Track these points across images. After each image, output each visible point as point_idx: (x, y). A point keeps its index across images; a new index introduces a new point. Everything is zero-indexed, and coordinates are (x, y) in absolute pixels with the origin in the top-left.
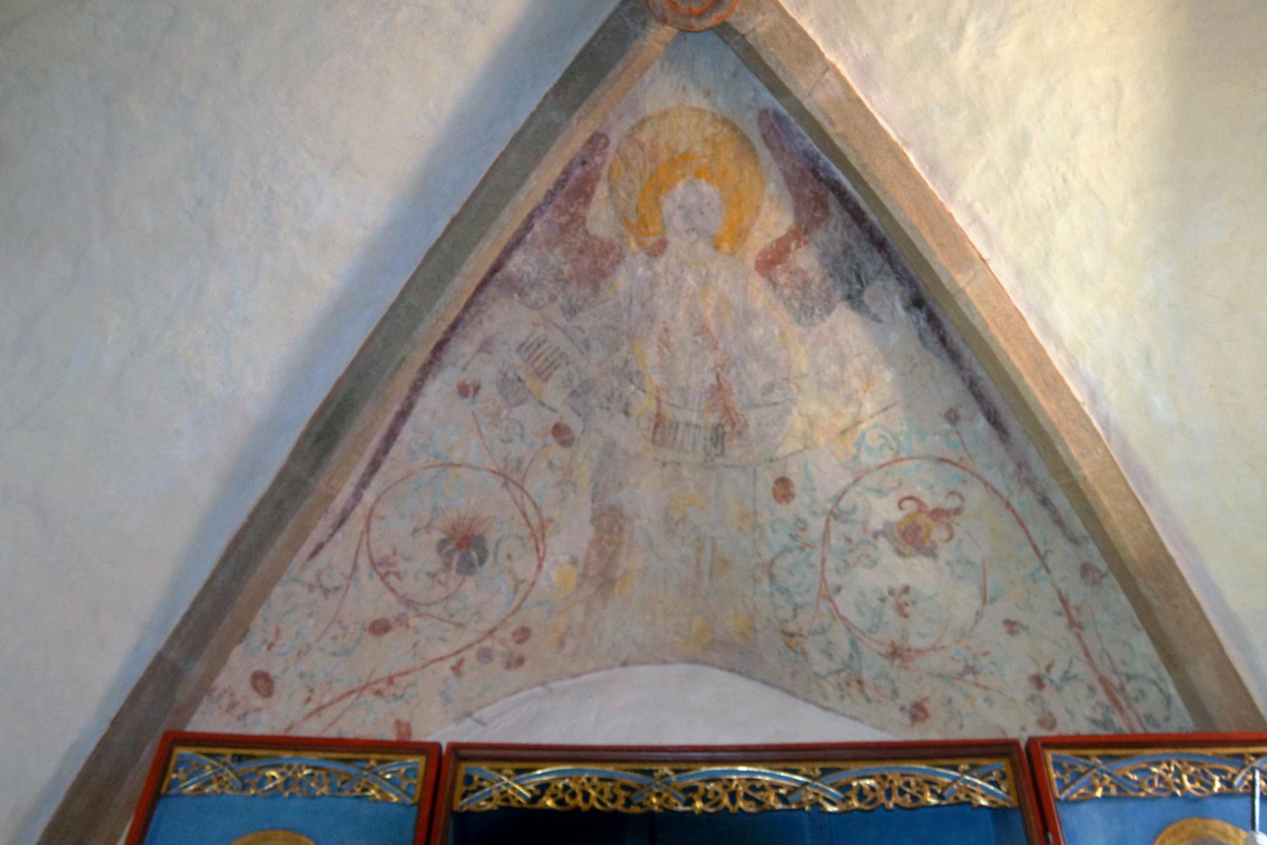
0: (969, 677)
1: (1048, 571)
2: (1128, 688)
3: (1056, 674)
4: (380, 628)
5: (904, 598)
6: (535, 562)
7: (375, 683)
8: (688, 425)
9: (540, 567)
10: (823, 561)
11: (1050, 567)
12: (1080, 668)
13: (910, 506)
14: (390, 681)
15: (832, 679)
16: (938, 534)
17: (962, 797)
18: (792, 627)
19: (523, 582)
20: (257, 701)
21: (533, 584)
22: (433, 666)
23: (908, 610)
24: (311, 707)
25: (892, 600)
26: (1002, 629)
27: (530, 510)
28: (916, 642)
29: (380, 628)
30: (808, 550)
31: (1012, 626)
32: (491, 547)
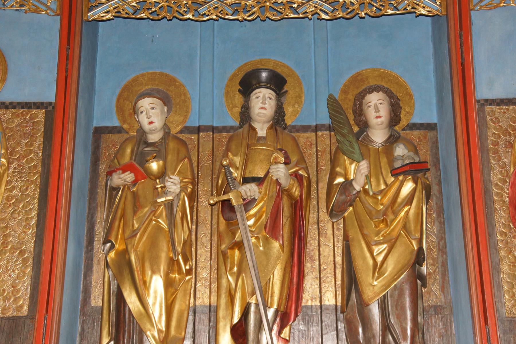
17: (409, 8)
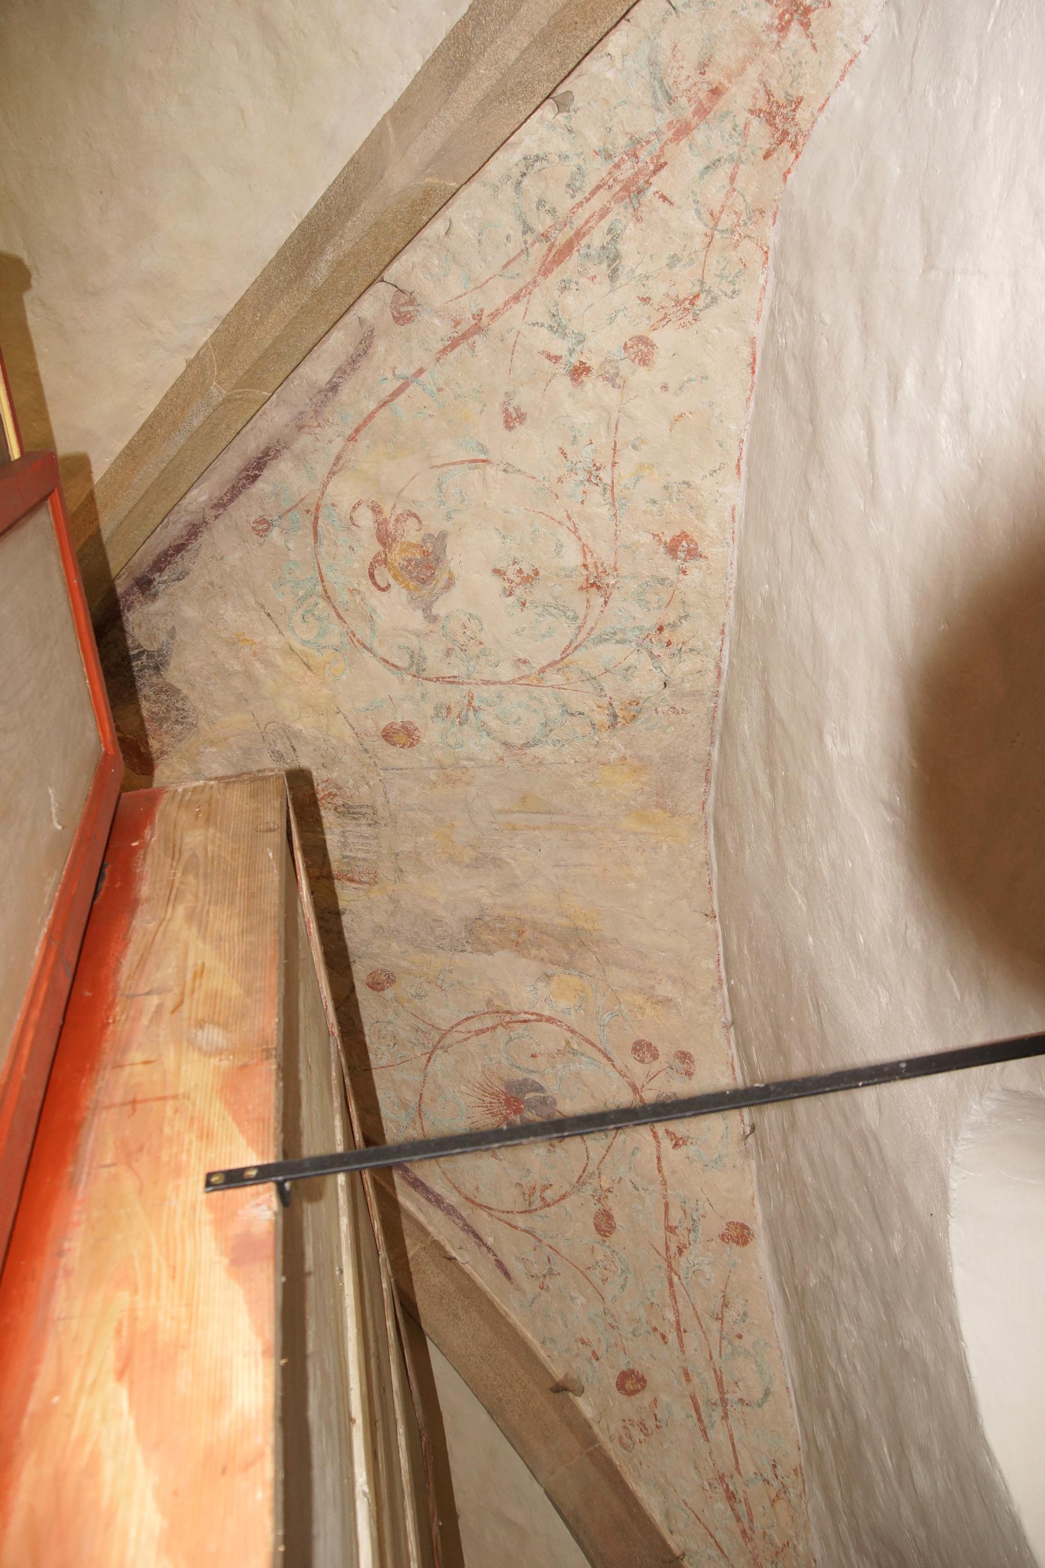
0: (605, 476)
1: (421, 371)
2: (540, 229)
3: (559, 346)
4: (605, 1224)
5: (511, 574)
6: (545, 1026)
7: (667, 1249)
8: (345, 845)
9: (550, 1020)
10: (486, 683)
11: (413, 371)
12: (537, 306)
13: (383, 576)
14: (670, 1229)
15: (666, 666)
16: (412, 534)
18: (602, 717)
19: (568, 1043)
20: (645, 1399)
21: (573, 1032)
22: (666, 1171)
23: (527, 570)
24: (672, 1337)
25: (518, 591)
26: (520, 430)
27: (476, 1025)
28: (572, 558)
29: (605, 1224)
30: (476, 703)
31: (513, 419)
32: (520, 1075)
